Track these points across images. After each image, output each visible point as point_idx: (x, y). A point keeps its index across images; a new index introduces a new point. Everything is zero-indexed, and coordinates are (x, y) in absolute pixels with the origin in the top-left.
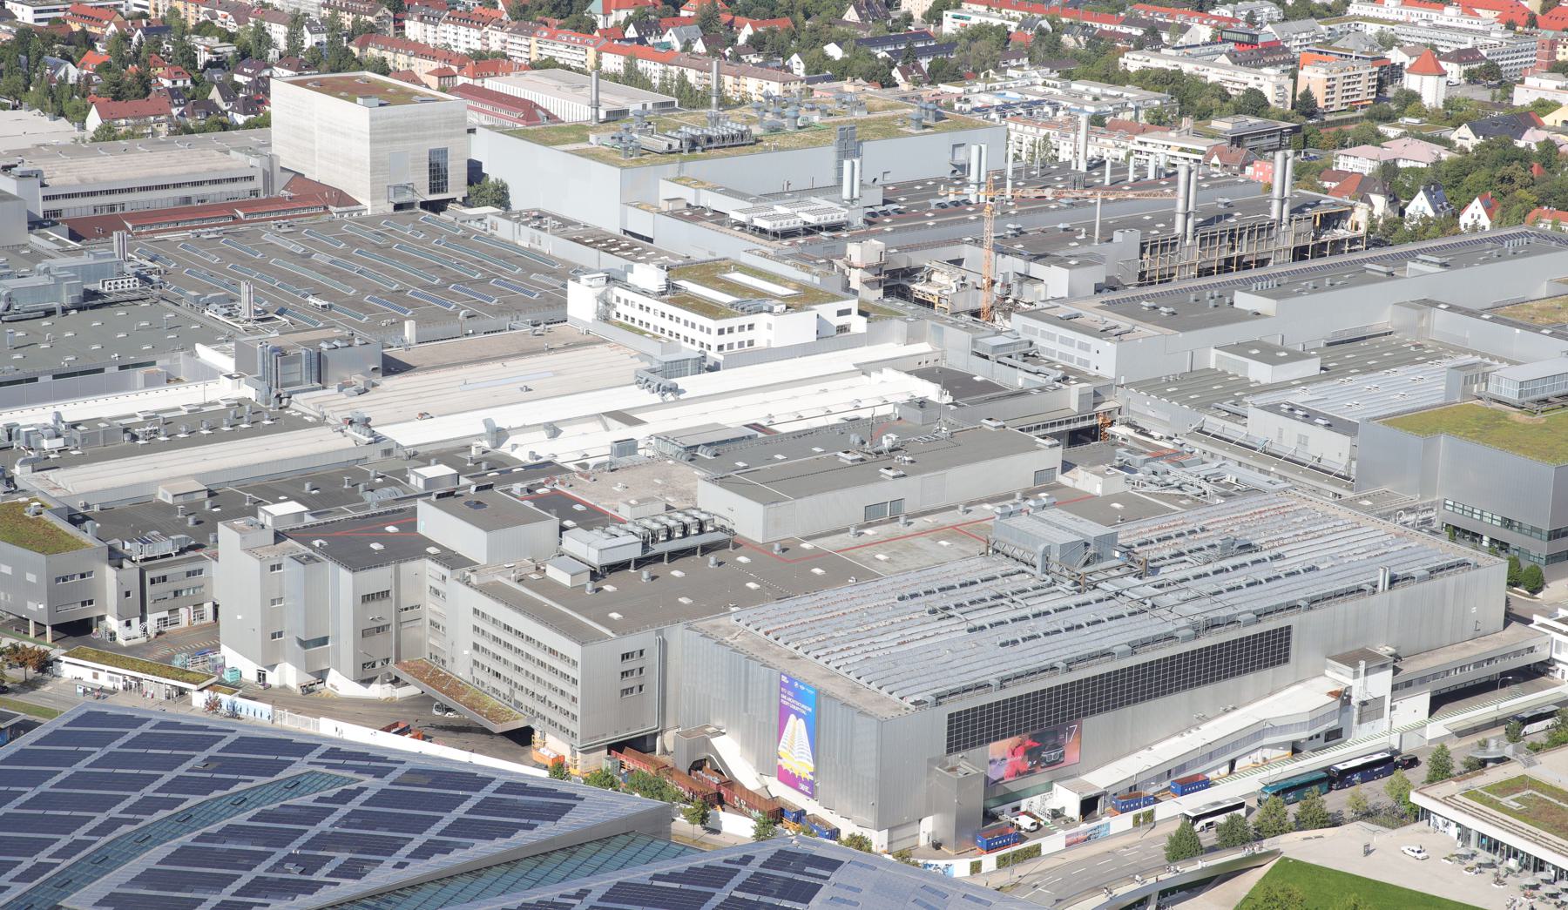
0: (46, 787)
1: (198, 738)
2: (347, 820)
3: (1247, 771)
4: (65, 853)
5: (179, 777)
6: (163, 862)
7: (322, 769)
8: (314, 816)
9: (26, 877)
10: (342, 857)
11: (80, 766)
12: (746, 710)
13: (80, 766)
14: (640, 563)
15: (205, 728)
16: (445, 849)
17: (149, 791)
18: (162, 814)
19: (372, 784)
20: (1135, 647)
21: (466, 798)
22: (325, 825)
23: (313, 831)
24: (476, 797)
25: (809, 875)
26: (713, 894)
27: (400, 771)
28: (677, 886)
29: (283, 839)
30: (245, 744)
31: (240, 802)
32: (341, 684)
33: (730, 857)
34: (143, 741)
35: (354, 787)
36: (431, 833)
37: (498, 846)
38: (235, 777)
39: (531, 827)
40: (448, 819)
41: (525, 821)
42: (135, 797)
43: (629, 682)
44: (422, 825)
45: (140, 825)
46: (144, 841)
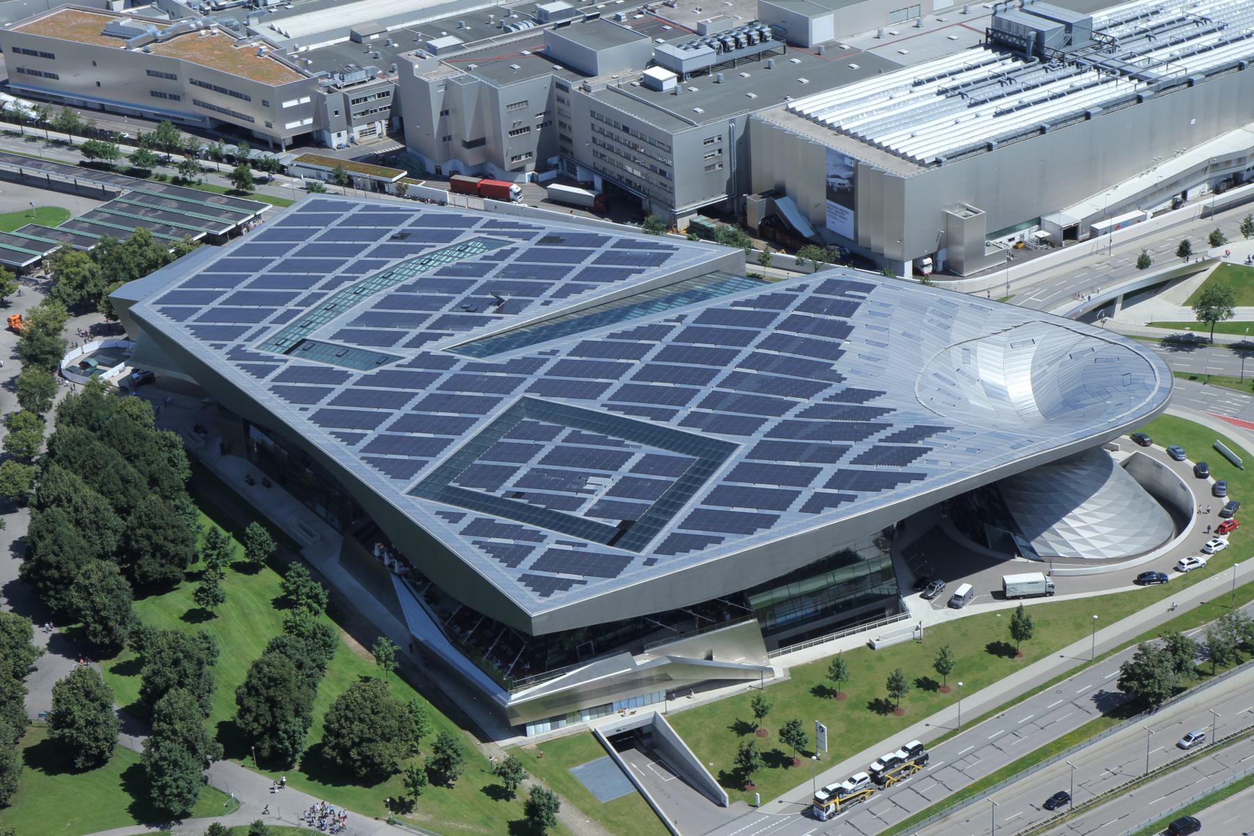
2: (505, 272)
3: (1195, 201)
4: (306, 303)
6: (376, 306)
8: (481, 269)
9: (281, 320)
11: (311, 240)
13: (311, 240)
14: (716, 67)
15: (398, 209)
16: (578, 290)
17: (361, 256)
18: (372, 272)
19: (523, 245)
21: (591, 252)
22: (490, 276)
23: (481, 281)
24: (599, 251)
25: (847, 296)
28: (752, 309)
29: (459, 287)
33: (790, 286)
35: (508, 247)
36: (568, 279)
40: (579, 268)
42: (352, 261)
44: (560, 273)
46: (358, 293)
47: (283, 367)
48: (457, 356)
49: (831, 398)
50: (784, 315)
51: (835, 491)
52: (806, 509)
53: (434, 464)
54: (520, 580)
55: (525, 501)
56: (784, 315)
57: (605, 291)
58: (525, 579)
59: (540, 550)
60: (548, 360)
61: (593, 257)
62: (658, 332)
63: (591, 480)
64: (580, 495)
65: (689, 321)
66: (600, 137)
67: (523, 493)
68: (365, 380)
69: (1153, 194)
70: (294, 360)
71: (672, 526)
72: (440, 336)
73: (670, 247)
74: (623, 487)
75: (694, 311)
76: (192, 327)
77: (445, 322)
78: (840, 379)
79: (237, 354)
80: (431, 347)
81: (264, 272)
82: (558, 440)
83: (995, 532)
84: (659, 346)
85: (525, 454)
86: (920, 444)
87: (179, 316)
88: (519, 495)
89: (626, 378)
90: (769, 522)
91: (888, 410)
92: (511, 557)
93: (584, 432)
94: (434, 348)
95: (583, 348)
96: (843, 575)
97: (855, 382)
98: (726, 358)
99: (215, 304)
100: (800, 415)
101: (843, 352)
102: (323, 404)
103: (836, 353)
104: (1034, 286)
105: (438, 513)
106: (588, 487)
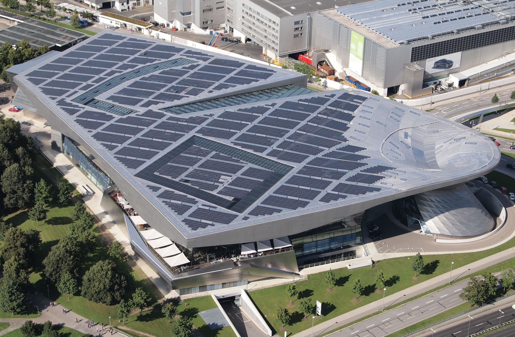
0: (91, 59)
1: (143, 44)
2: (192, 76)
4: (97, 81)
5: (136, 58)
6: (129, 86)
7: (185, 57)
8: (181, 73)
10: (191, 88)
11: (103, 52)
12: (339, 44)
13: (103, 52)
15: (145, 41)
16: (226, 87)
17: (125, 62)
18: (129, 70)
19: (202, 64)
20: (484, 26)
21: (235, 70)
22: (185, 77)
23: (181, 78)
24: (238, 70)
26: (320, 107)
27: (212, 59)
28: (307, 103)
29: (171, 81)
30: (159, 47)
31: (156, 67)
32: (196, 29)
33: (326, 94)
34: (124, 44)
35: (195, 64)
37: (245, 87)
38: (155, 58)
39: (257, 81)
40: (228, 76)
41: (255, 79)
42: (121, 64)
43: (297, 32)
45: (122, 73)
46: (123, 79)
47: (82, 111)
48: (165, 113)
49: (340, 149)
50: (322, 108)
51: (337, 193)
52: (323, 200)
53: (149, 162)
54: (183, 221)
55: (189, 184)
56: (322, 108)
57: (240, 88)
58: (185, 221)
59: (194, 208)
60: (208, 118)
61: (235, 72)
62: (262, 110)
63: (222, 177)
64: (216, 184)
65: (277, 107)
66: (245, 16)
67: (189, 181)
68: (120, 121)
69: (503, 68)
70: (88, 108)
71: (258, 203)
72: (158, 103)
73: (272, 71)
74: (237, 182)
75: (280, 102)
76: (42, 88)
77: (162, 97)
78: (345, 140)
79: (61, 103)
80: (154, 108)
81: (79, 65)
82: (208, 157)
83: (411, 220)
84: (261, 117)
85: (192, 162)
86: (379, 175)
87: (36, 82)
88: (187, 181)
89: (244, 131)
90: (304, 204)
91: (366, 157)
92: (180, 210)
93: (221, 154)
94: (154, 108)
95: (226, 115)
96: (338, 234)
97: (352, 143)
98: (292, 125)
99: (54, 78)
100: (325, 155)
101: (349, 128)
102: (99, 130)
103: (345, 128)
104: (443, 106)
105: (148, 186)
106: (220, 180)
